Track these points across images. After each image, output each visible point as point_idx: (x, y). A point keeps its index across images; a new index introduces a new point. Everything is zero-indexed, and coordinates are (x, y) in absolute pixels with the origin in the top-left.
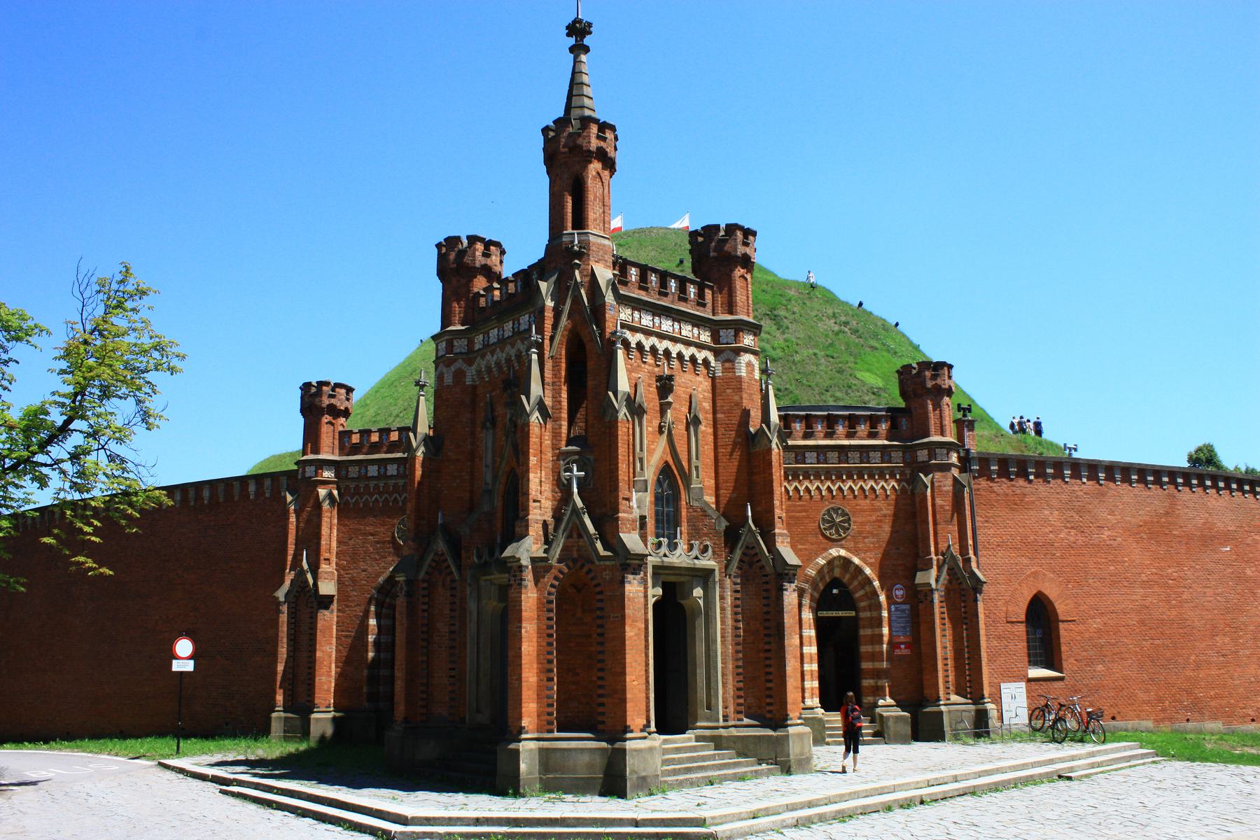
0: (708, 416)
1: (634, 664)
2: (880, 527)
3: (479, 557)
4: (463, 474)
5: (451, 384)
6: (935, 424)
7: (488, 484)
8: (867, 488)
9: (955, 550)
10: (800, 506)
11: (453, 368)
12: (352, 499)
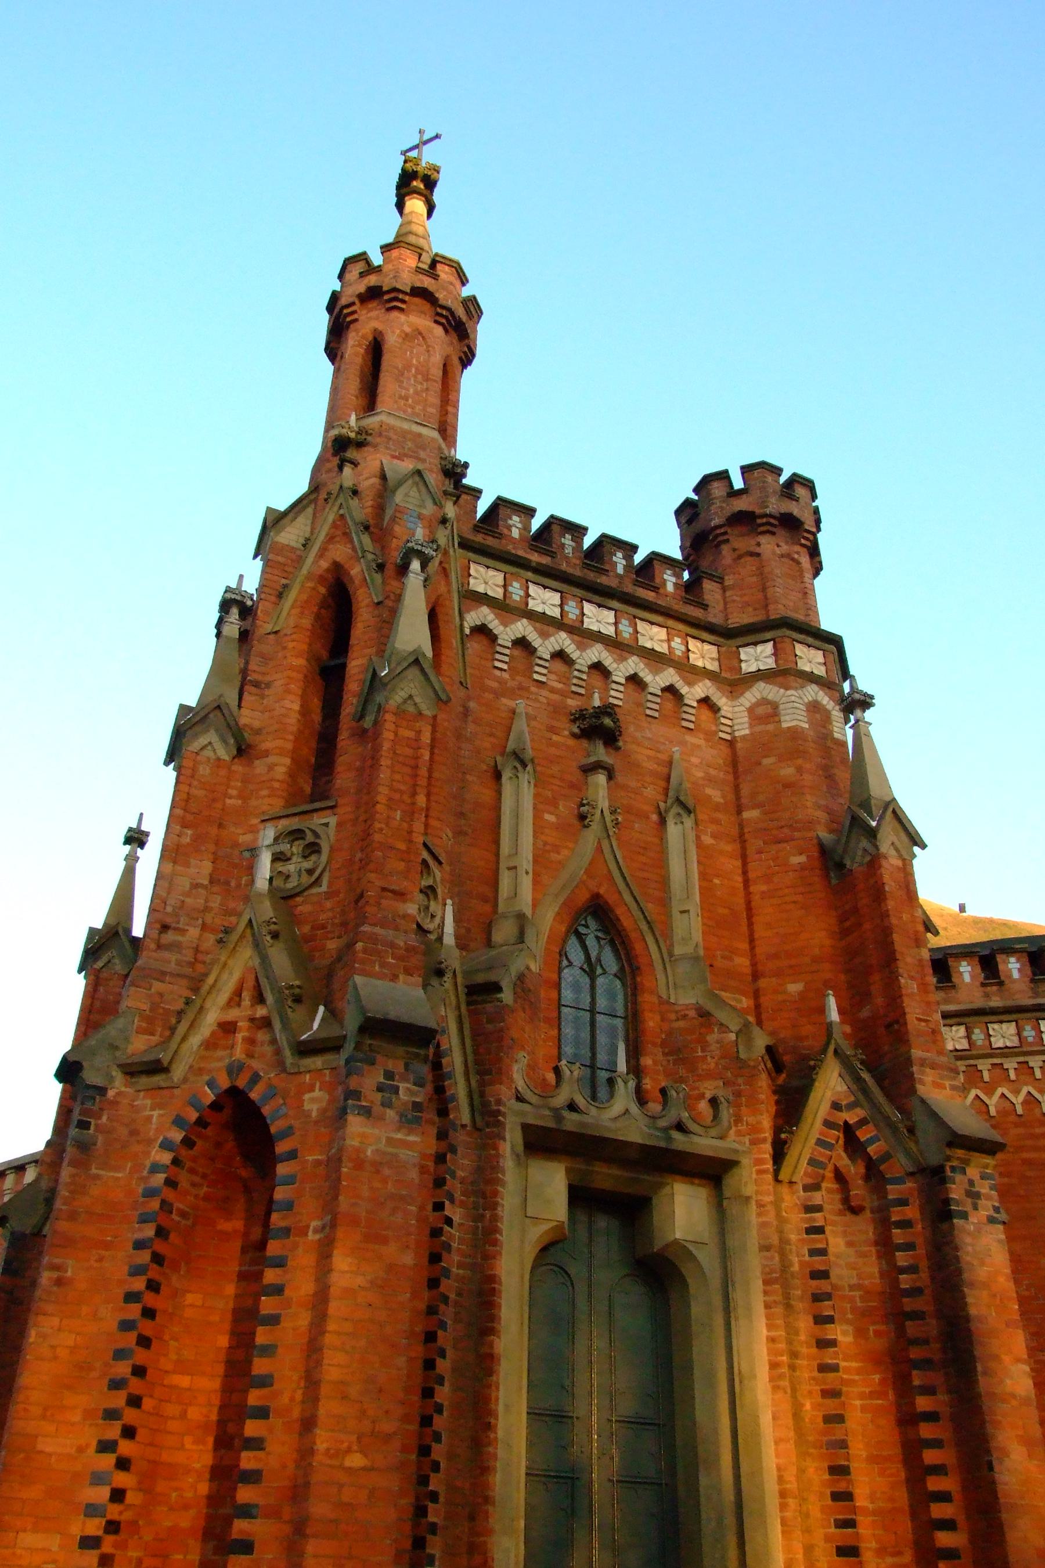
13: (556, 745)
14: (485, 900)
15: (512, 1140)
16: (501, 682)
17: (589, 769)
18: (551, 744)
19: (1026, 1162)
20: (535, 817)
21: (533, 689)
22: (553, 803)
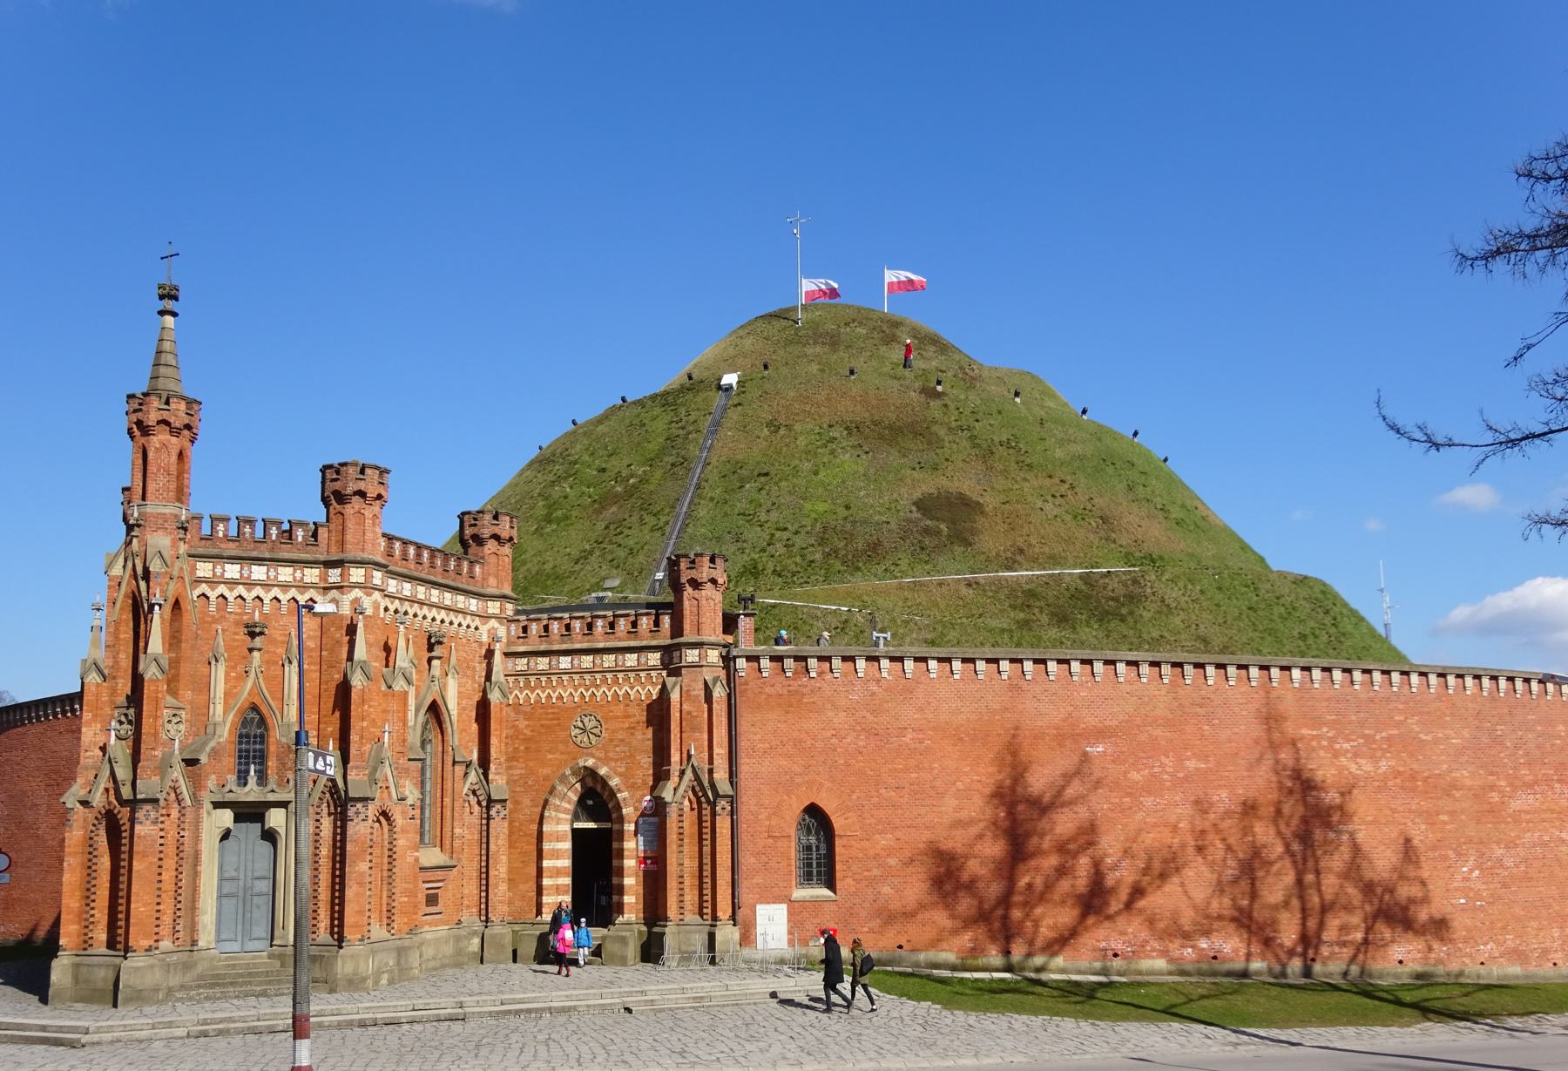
0: (313, 654)
1: (141, 894)
2: (632, 734)
6: (692, 621)
8: (620, 693)
9: (699, 759)
10: (553, 713)
13: (237, 640)
14: (204, 715)
15: (207, 806)
16: (213, 617)
17: (251, 650)
18: (235, 640)
19: (542, 726)
20: (225, 675)
21: (227, 616)
22: (234, 667)
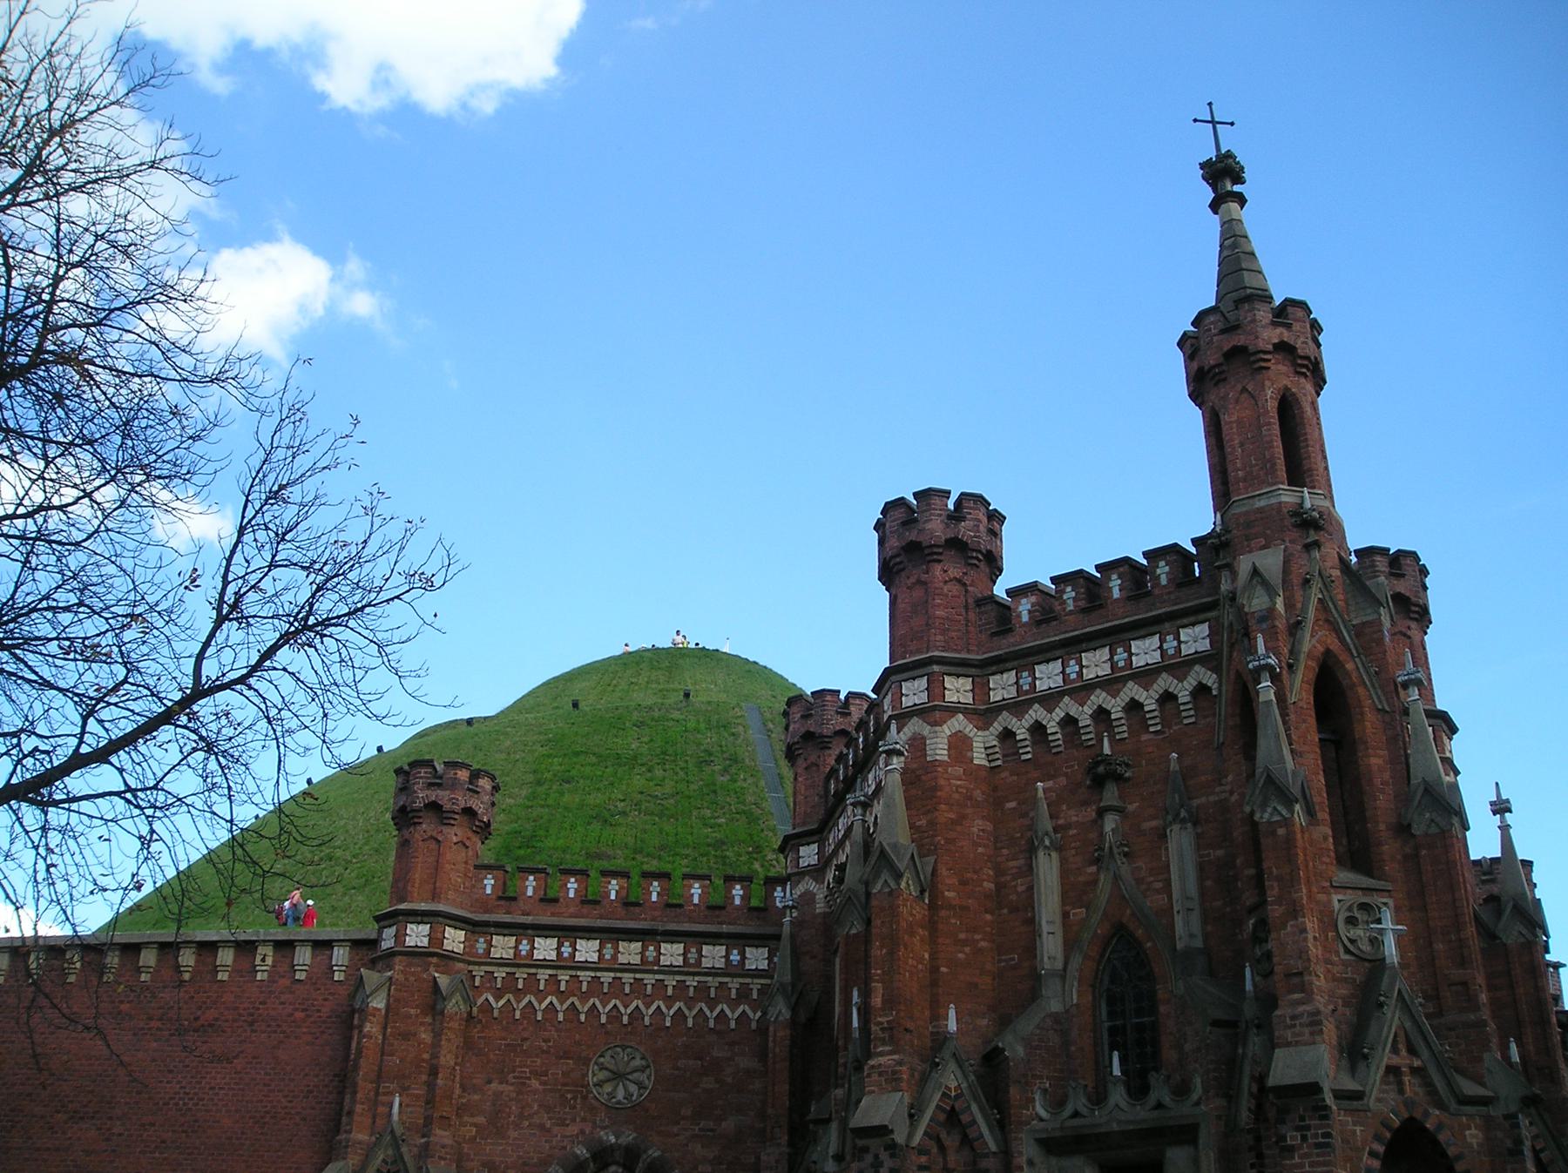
3: (1057, 1103)
4: (977, 937)
5: (946, 758)
7: (1055, 958)
11: (947, 730)
12: (497, 999)
